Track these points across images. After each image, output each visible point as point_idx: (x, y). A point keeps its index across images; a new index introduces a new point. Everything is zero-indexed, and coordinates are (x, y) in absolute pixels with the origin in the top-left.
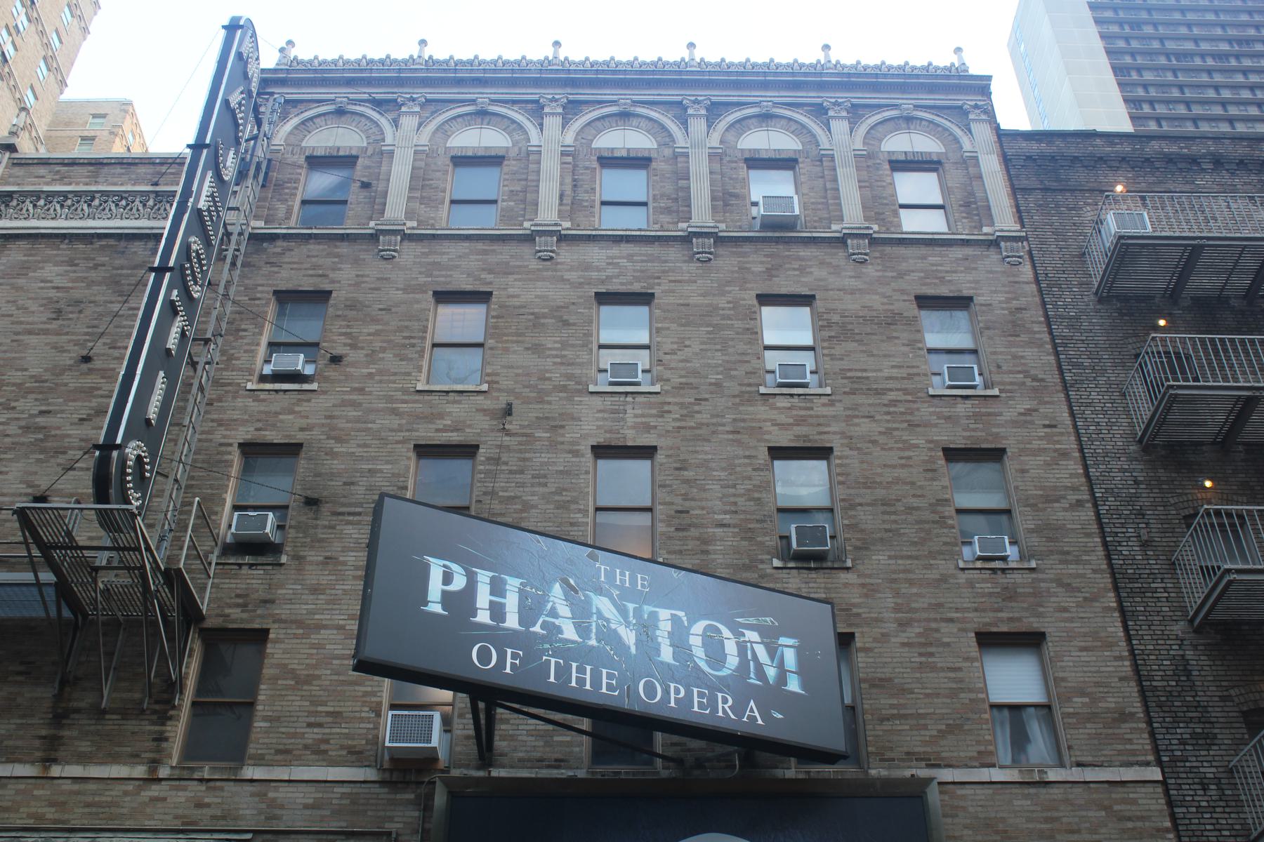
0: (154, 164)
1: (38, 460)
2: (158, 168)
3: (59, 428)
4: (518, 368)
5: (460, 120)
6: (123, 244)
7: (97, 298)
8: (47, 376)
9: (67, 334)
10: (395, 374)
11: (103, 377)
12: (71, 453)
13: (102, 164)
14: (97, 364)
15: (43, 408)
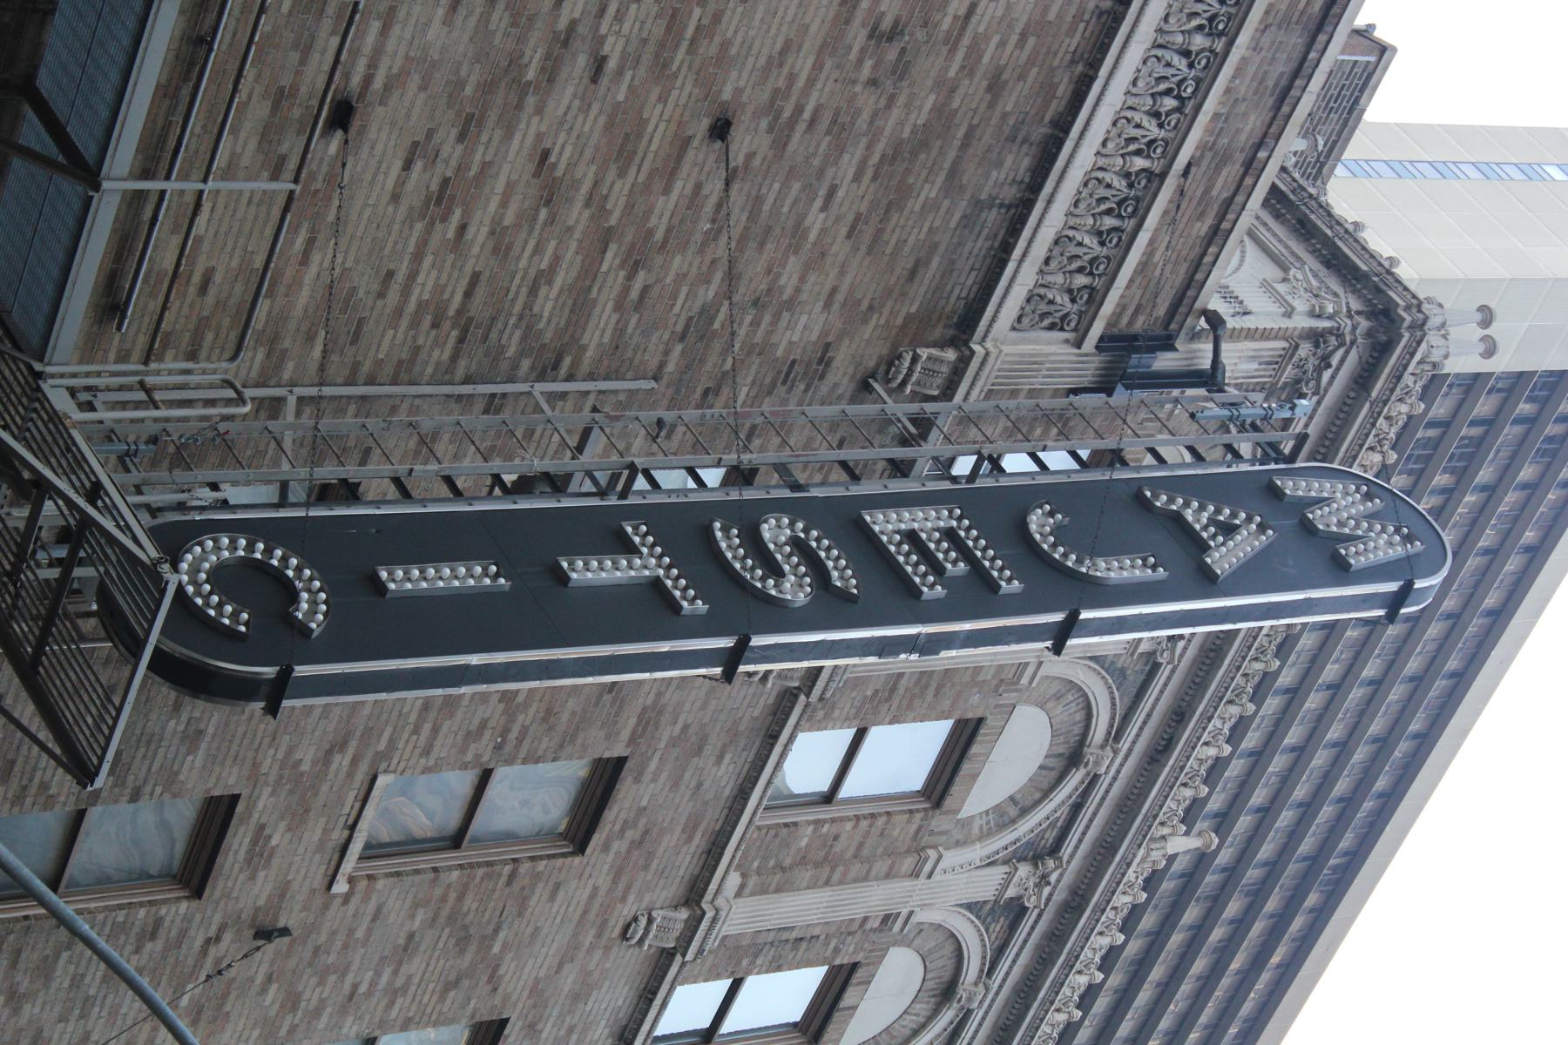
0: (1259, 146)
1: (461, 84)
2: (1240, 158)
3: (539, 110)
4: (369, 931)
5: (1079, 716)
6: (1041, 131)
7: (896, 112)
8: (708, 49)
9: (818, 66)
10: (435, 730)
11: (653, 172)
12: (451, 151)
13: (1319, 28)
14: (702, 155)
15: (612, 64)
